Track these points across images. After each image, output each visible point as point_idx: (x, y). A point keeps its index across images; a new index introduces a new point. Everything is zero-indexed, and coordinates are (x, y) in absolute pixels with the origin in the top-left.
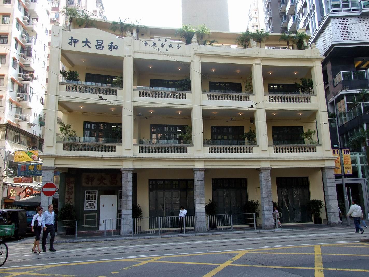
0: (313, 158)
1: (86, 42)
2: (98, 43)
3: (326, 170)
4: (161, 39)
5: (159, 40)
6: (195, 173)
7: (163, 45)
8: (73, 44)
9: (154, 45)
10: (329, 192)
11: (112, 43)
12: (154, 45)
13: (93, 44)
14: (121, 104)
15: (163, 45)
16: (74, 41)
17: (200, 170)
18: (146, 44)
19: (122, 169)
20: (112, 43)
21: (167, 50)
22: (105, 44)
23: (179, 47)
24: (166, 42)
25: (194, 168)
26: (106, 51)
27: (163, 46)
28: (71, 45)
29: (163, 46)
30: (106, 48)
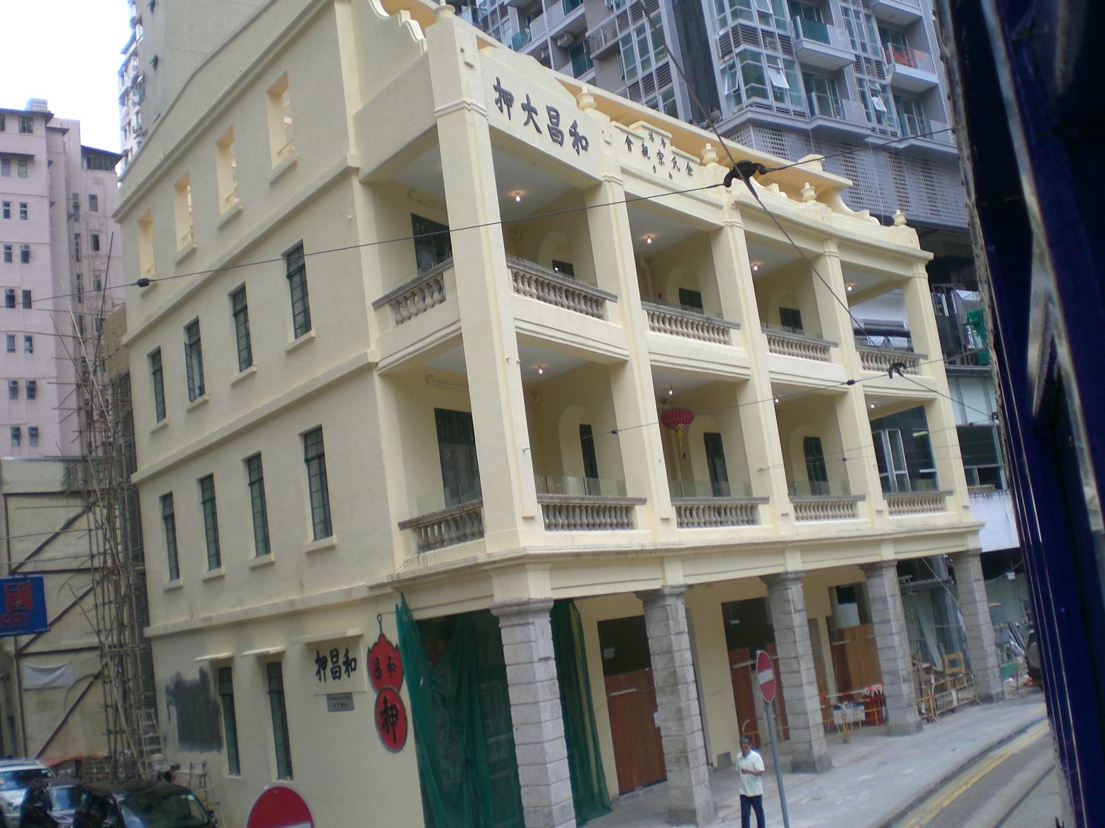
0: (956, 528)
1: (528, 108)
2: (551, 117)
3: (970, 559)
4: (654, 136)
5: (652, 138)
6: (787, 589)
7: (660, 155)
8: (505, 107)
9: (645, 152)
10: (980, 616)
11: (575, 126)
12: (645, 152)
13: (543, 120)
14: (626, 353)
15: (660, 155)
16: (505, 99)
17: (799, 577)
18: (629, 142)
19: (667, 591)
20: (575, 126)
21: (671, 176)
22: (565, 127)
23: (689, 170)
24: (664, 146)
25: (787, 573)
26: (565, 153)
27: (661, 159)
28: (502, 111)
29: (661, 159)
30: (569, 140)
